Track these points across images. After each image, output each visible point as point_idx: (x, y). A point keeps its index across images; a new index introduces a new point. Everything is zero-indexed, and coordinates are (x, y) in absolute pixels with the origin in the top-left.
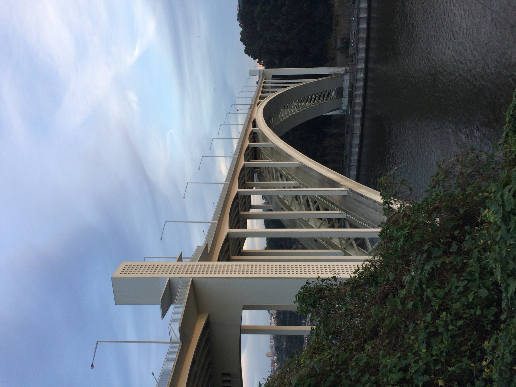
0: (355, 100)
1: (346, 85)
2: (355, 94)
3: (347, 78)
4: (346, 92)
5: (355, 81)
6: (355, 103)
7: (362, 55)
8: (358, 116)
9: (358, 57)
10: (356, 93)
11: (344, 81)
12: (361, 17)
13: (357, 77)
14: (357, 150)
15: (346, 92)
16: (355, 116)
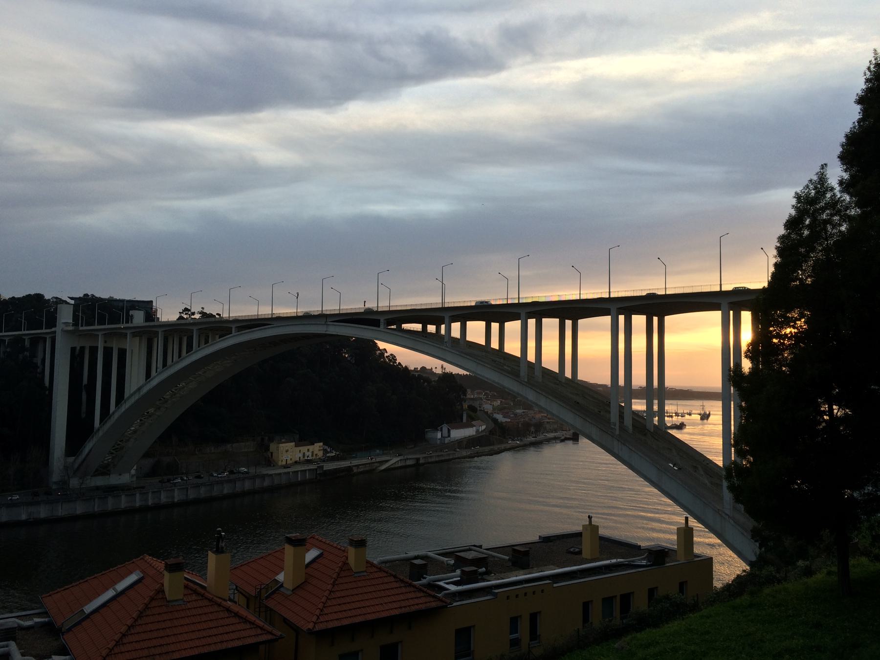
0: (126, 495)
1: (114, 480)
2: (135, 494)
3: (125, 479)
4: (100, 481)
5: (156, 490)
6: (121, 496)
7: (192, 494)
8: (96, 507)
9: (189, 488)
10: (138, 495)
11: (120, 475)
12: (235, 484)
13: (162, 491)
14: (24, 517)
15: (100, 481)
16: (96, 500)
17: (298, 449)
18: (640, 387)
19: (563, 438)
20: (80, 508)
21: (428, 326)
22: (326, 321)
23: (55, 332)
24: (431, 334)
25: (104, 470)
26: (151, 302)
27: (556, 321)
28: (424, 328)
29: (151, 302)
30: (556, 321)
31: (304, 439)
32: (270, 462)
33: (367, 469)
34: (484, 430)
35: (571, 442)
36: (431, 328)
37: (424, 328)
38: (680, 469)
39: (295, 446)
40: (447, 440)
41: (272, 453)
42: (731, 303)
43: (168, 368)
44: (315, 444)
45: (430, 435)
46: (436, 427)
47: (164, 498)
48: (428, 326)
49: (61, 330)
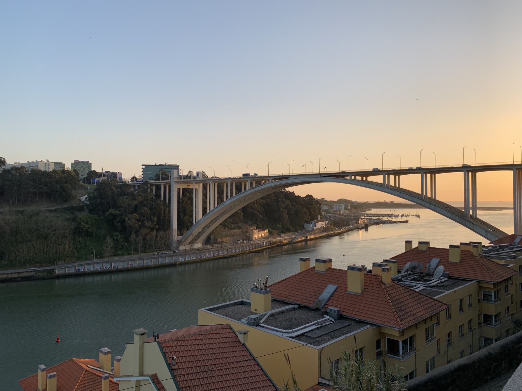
17: (260, 232)
18: (375, 202)
19: (360, 227)
20: (193, 258)
21: (357, 177)
22: (321, 177)
23: (170, 182)
24: (364, 181)
25: (192, 243)
26: (178, 166)
27: (430, 175)
28: (362, 178)
29: (178, 166)
30: (430, 175)
31: (260, 228)
32: (249, 238)
33: (288, 241)
34: (328, 223)
35: (363, 230)
36: (364, 178)
37: (362, 178)
38: (493, 231)
39: (259, 231)
40: (315, 228)
41: (249, 234)
42: (516, 169)
43: (234, 197)
44: (265, 230)
45: (306, 226)
46: (308, 222)
48: (357, 177)
49: (174, 181)
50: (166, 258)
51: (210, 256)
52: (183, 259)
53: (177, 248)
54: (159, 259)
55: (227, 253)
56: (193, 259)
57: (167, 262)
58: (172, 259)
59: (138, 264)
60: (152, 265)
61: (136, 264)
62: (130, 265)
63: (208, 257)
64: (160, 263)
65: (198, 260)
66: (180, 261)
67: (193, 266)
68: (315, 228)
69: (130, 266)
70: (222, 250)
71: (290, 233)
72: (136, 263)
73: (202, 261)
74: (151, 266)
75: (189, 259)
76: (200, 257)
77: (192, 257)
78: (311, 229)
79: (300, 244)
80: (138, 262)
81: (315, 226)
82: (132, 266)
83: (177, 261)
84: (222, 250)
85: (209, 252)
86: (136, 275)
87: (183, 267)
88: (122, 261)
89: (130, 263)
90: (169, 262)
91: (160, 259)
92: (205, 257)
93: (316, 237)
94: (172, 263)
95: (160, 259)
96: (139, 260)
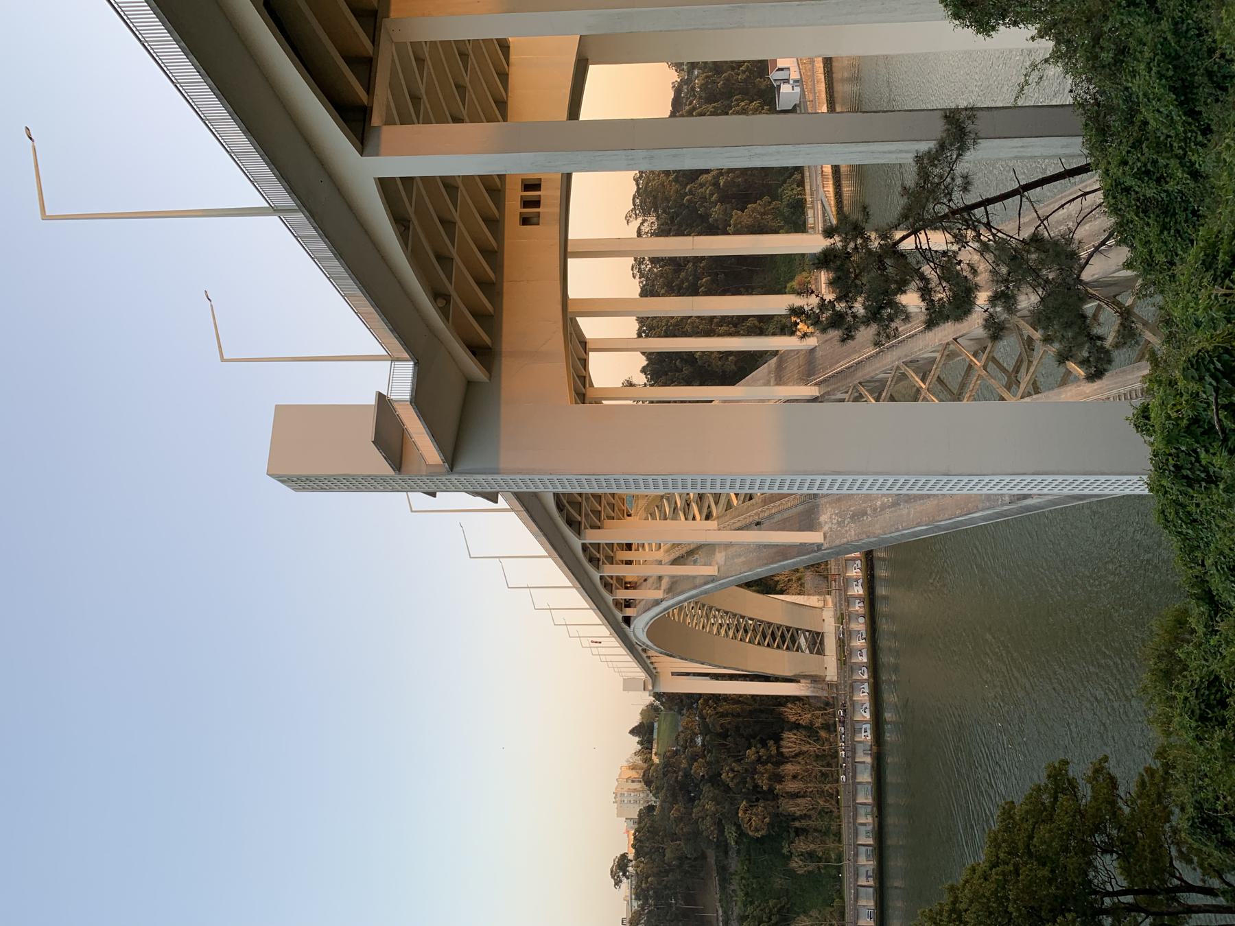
4: (830, 644)
15: (830, 644)
25: (816, 642)
47: (858, 590)
50: (859, 783)
51: (864, 632)
52: (864, 726)
53: (830, 685)
54: (860, 804)
55: (859, 562)
56: (867, 690)
57: (870, 780)
58: (864, 762)
59: (868, 856)
60: (874, 821)
61: (866, 863)
62: (868, 877)
63: (864, 636)
64: (870, 800)
65: (872, 680)
66: (868, 733)
67: (890, 697)
68: (795, 75)
69: (870, 877)
70: (847, 582)
71: (809, 199)
72: (864, 865)
73: (875, 666)
74: (876, 829)
75: (867, 705)
76: (864, 668)
77: (862, 695)
78: (797, 90)
79: (846, 190)
80: (862, 860)
81: (789, 69)
82: (870, 873)
83: (869, 748)
84: (847, 582)
85: (850, 633)
86: (896, 863)
87: (888, 727)
88: (857, 898)
89: (862, 881)
90: (869, 770)
91: (860, 799)
92: (864, 651)
93: (824, 95)
94: (873, 767)
95: (860, 799)
96: (856, 855)
